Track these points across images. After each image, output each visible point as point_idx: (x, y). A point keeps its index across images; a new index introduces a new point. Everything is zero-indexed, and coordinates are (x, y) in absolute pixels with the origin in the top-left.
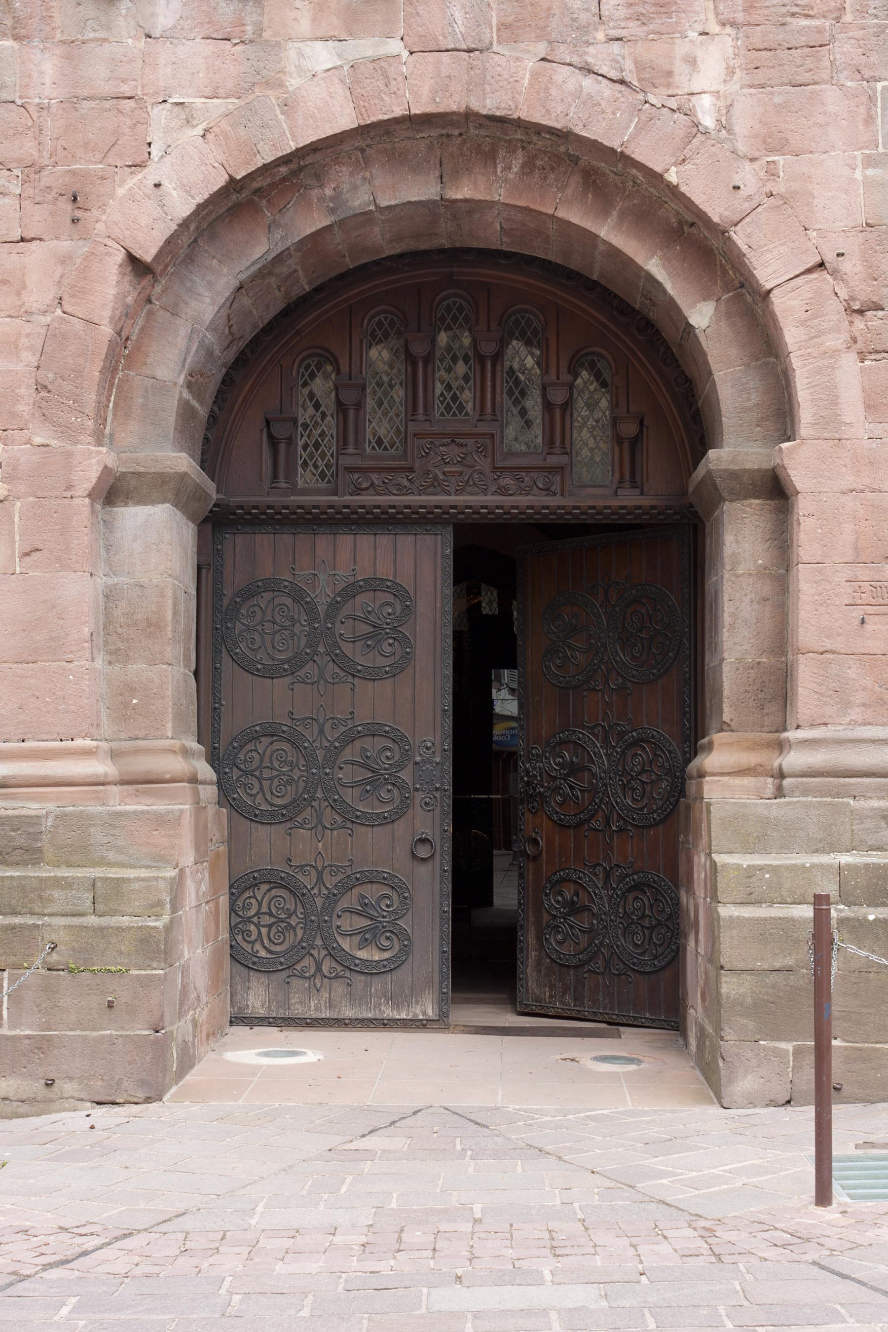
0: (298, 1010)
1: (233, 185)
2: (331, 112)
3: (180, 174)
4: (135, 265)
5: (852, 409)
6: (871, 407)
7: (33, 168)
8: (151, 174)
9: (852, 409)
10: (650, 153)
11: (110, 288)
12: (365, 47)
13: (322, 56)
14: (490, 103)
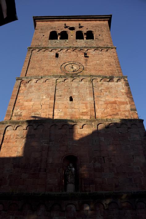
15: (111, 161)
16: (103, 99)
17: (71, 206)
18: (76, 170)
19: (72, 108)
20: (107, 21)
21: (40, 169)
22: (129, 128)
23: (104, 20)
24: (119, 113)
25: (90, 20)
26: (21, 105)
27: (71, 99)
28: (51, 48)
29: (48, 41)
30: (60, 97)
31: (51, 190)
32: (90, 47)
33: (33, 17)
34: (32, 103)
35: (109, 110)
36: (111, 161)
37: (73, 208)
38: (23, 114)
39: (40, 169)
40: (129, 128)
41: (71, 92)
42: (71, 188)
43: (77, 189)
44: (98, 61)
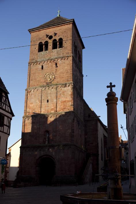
18: (49, 136)
19: (48, 107)
20: (72, 24)
22: (68, 116)
23: (70, 24)
24: (66, 107)
25: (61, 26)
27: (48, 101)
28: (39, 61)
29: (37, 54)
32: (59, 58)
33: (28, 30)
34: (33, 105)
35: (62, 106)
36: (59, 132)
37: (47, 150)
38: (30, 112)
40: (68, 116)
41: (48, 97)
42: (47, 142)
44: (62, 69)
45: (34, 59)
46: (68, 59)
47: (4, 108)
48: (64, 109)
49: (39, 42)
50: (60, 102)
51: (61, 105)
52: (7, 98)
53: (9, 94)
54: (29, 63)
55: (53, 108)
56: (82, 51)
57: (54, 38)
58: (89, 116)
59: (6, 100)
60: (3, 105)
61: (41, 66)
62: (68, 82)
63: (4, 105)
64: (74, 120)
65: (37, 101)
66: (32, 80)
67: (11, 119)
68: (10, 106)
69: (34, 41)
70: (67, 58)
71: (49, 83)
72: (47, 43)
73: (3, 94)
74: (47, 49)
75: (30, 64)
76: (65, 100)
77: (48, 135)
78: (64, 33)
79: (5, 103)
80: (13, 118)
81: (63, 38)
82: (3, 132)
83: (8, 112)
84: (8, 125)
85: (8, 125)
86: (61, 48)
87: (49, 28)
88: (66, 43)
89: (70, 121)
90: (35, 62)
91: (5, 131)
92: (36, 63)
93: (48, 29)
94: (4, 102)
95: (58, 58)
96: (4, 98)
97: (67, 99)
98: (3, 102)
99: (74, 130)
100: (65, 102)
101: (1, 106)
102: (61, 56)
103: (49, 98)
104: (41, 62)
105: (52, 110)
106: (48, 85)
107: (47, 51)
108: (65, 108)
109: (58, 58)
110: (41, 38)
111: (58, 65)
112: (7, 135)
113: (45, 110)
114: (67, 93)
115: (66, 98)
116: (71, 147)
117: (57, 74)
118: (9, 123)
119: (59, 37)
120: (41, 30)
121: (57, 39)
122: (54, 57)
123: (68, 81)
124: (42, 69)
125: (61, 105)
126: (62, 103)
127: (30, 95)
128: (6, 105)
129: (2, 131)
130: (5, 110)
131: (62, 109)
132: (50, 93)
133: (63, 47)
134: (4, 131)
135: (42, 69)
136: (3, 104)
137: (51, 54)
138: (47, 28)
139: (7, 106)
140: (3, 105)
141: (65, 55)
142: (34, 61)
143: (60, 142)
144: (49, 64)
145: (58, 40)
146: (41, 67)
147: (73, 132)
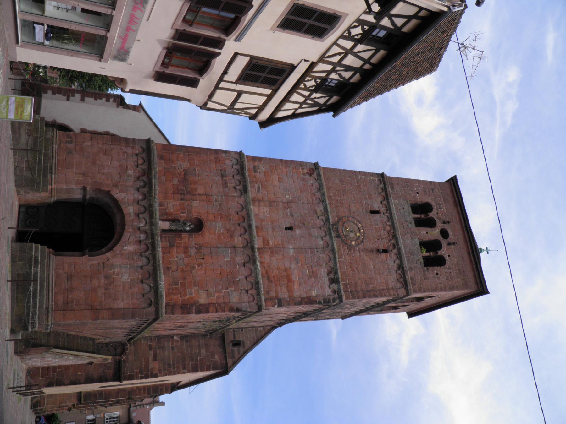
0: (21, 214)
1: (117, 201)
2: (125, 211)
3: (118, 195)
4: (109, 191)
5: (92, 262)
6: (92, 264)
7: (120, 182)
8: (119, 193)
9: (92, 262)
10: (120, 242)
11: (107, 189)
12: (132, 214)
13: (131, 210)
14: (126, 227)
15: (198, 266)
16: (293, 266)
17: (144, 222)
19: (273, 229)
21: (184, 194)
22: (247, 291)
23: (476, 283)
25: (471, 261)
26: (272, 172)
30: (289, 214)
31: (161, 205)
34: (277, 183)
35: (276, 271)
39: (184, 194)
40: (247, 291)
41: (299, 227)
42: (165, 225)
43: (164, 231)
44: (374, 267)
45: (393, 188)
46: (401, 282)
47: (296, 97)
48: (269, 278)
49: (433, 204)
50: (287, 264)
51: (278, 269)
52: (322, 109)
53: (334, 116)
54: (382, 175)
55: (271, 243)
56: (404, 311)
57: (444, 243)
58: (237, 344)
59: (316, 104)
60: (303, 96)
61: (377, 209)
62: (342, 288)
63: (302, 99)
64: (238, 310)
65: (287, 196)
66: (341, 181)
67: (253, 117)
68: (294, 116)
69: (432, 190)
70: (402, 280)
71: (337, 231)
72: (431, 223)
73: (335, 99)
74: (419, 223)
75: (380, 177)
76: (294, 279)
77: (188, 229)
78: (457, 268)
79: (308, 101)
80: (255, 123)
81: (445, 266)
82: (217, 87)
83: (278, 108)
84: (237, 106)
85: (236, 107)
86: (422, 261)
87: (465, 230)
88: (435, 275)
89: (234, 298)
90: (386, 192)
91: (220, 96)
92: (383, 194)
93: (462, 226)
94: (312, 99)
95: (399, 256)
96: (322, 101)
97: (296, 286)
98: (314, 95)
99: (208, 312)
100: (288, 282)
101: (302, 89)
102: (406, 265)
103: (298, 231)
104: (388, 209)
105: (265, 242)
106: (333, 227)
107: (413, 223)
108: (272, 282)
109: (399, 256)
110: (441, 208)
111: (383, 255)
112: (205, 100)
113: (262, 220)
114: (312, 286)
115: (300, 284)
116: (150, 305)
117: (362, 253)
118: (242, 109)
119: (446, 256)
120: (459, 207)
121: (444, 252)
122: (401, 244)
123: (346, 285)
124: (373, 212)
125: (278, 269)
126: (286, 270)
127: (304, 174)
128: (301, 104)
129: (222, 85)
130: (286, 99)
131: (267, 273)
132: (310, 235)
133: (425, 268)
134: (218, 91)
135: (373, 212)
136: (307, 93)
137: (409, 236)
138: (464, 225)
139: (297, 106)
140: (303, 96)
141: (409, 275)
142: (389, 189)
143: (168, 268)
144: (384, 229)
145: (440, 253)
146: (376, 208)
147: (198, 312)
